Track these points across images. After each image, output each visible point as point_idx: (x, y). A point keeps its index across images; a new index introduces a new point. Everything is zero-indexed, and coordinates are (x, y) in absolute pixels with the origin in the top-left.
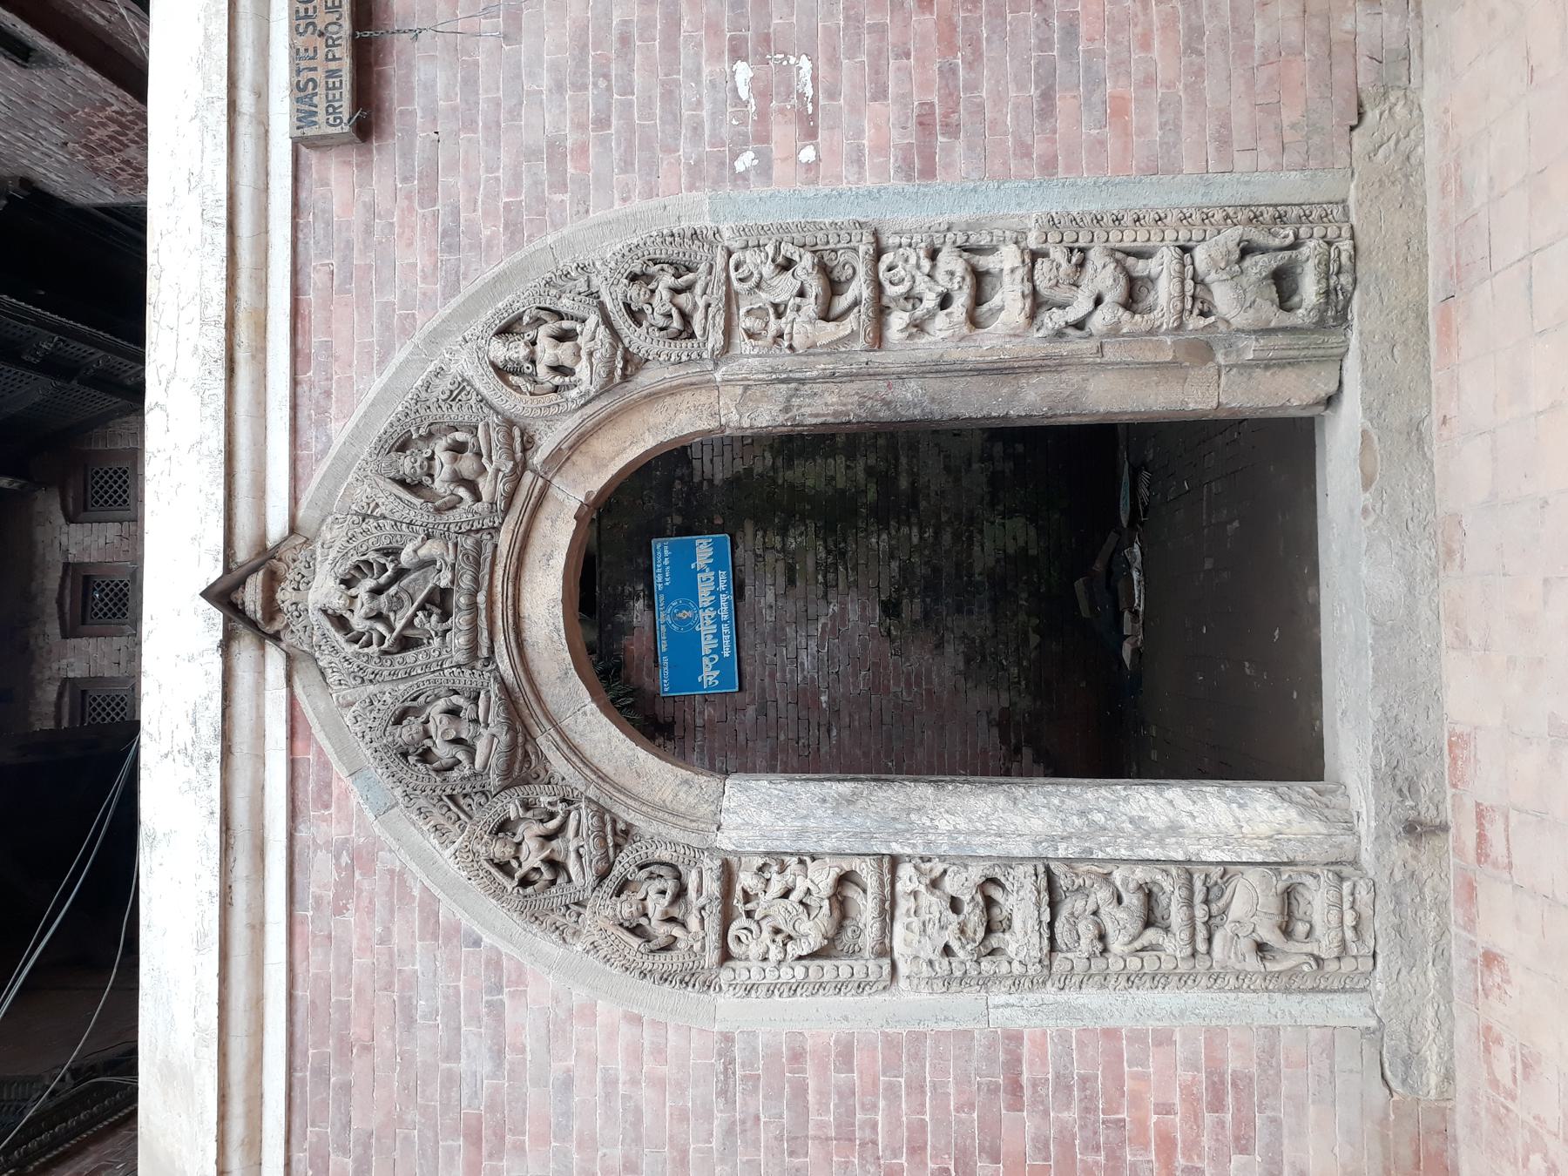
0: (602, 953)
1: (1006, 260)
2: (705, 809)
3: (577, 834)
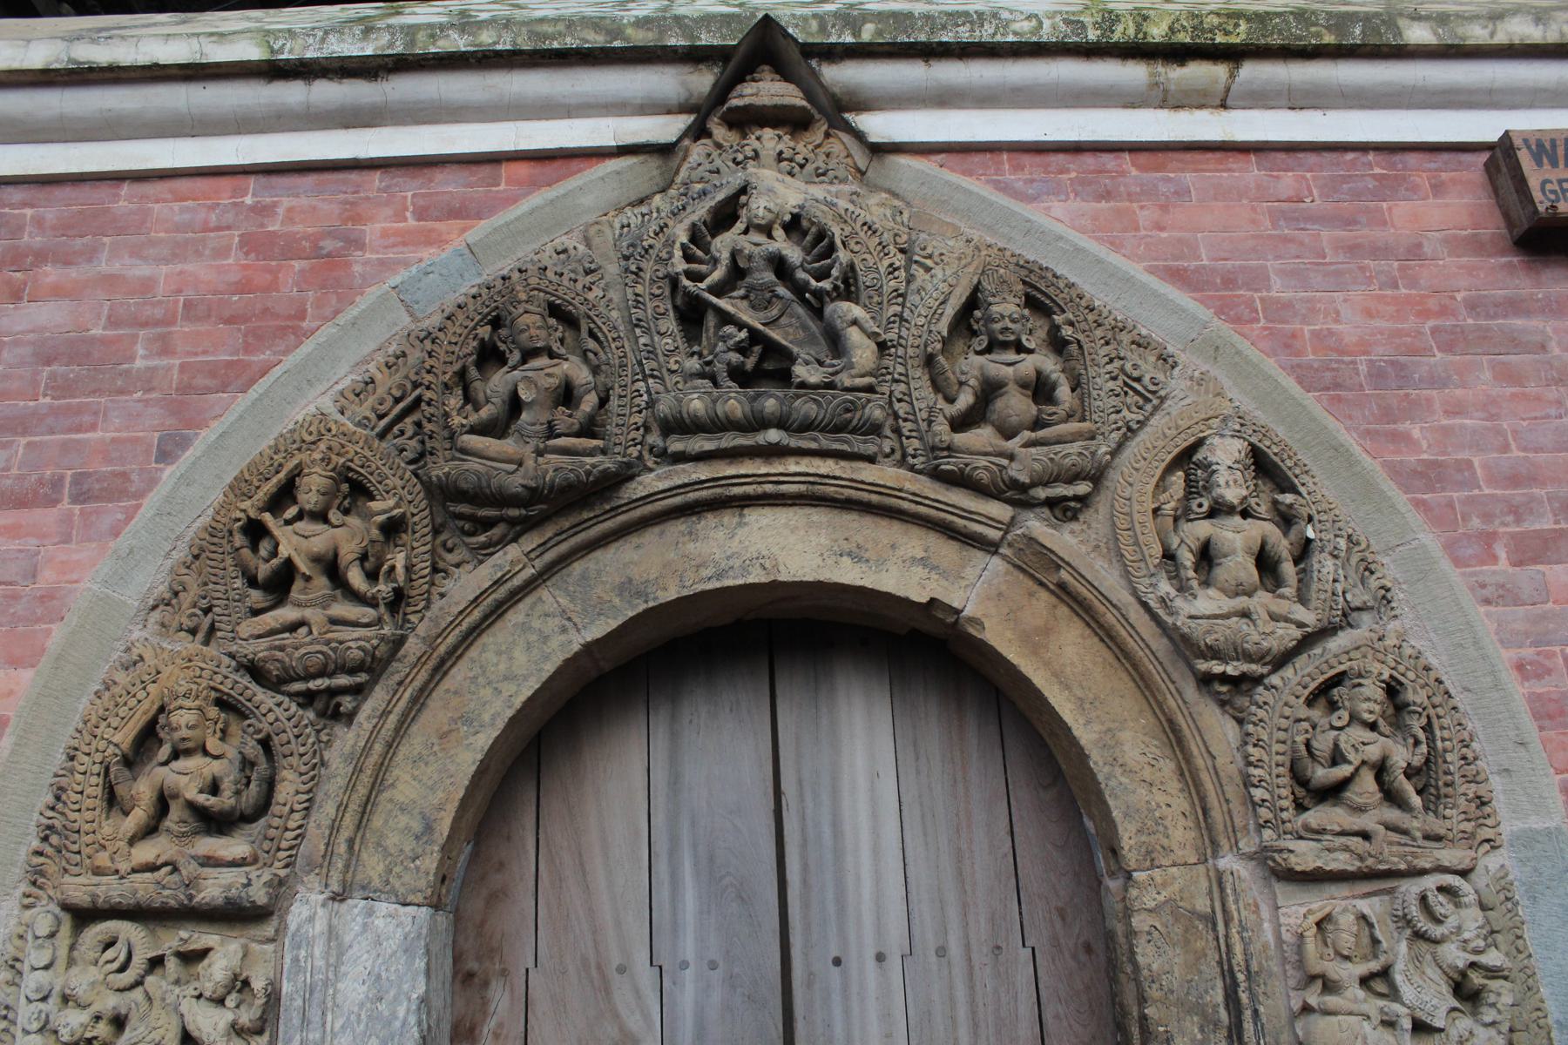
0: (122, 677)
2: (372, 866)
3: (334, 621)
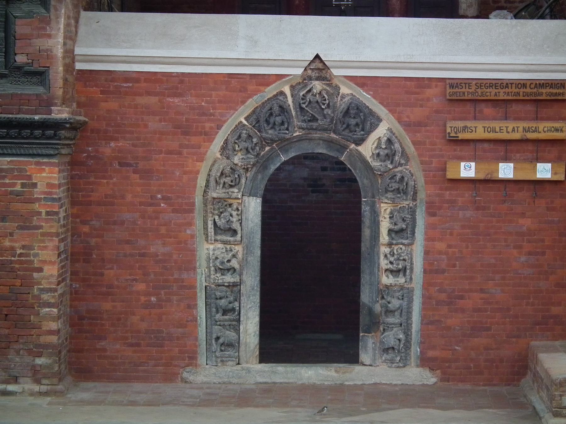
1: (401, 280)
